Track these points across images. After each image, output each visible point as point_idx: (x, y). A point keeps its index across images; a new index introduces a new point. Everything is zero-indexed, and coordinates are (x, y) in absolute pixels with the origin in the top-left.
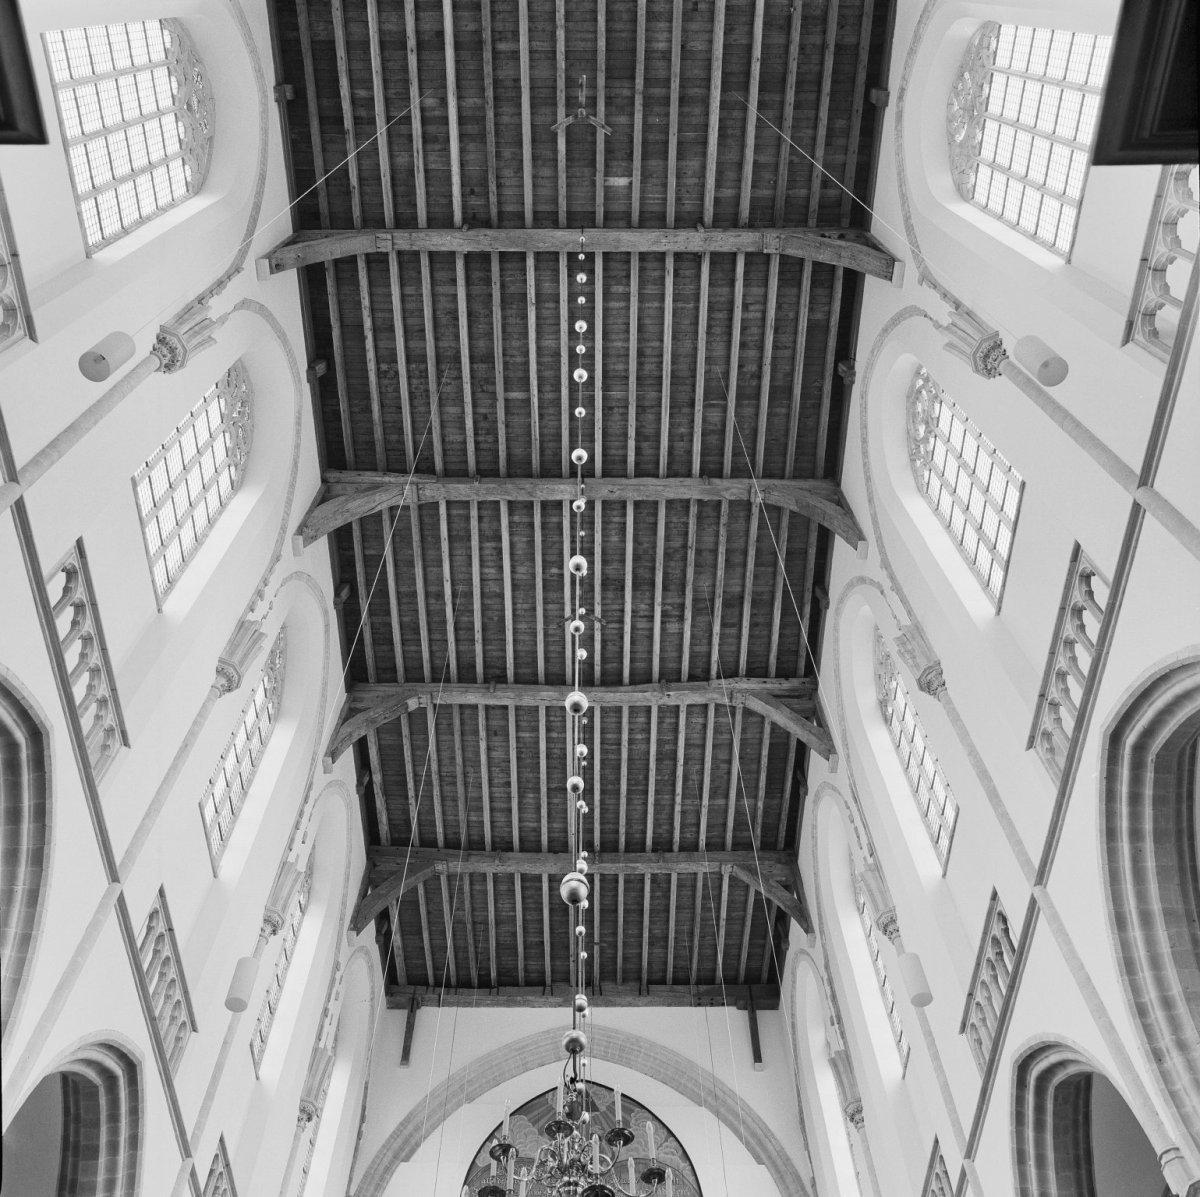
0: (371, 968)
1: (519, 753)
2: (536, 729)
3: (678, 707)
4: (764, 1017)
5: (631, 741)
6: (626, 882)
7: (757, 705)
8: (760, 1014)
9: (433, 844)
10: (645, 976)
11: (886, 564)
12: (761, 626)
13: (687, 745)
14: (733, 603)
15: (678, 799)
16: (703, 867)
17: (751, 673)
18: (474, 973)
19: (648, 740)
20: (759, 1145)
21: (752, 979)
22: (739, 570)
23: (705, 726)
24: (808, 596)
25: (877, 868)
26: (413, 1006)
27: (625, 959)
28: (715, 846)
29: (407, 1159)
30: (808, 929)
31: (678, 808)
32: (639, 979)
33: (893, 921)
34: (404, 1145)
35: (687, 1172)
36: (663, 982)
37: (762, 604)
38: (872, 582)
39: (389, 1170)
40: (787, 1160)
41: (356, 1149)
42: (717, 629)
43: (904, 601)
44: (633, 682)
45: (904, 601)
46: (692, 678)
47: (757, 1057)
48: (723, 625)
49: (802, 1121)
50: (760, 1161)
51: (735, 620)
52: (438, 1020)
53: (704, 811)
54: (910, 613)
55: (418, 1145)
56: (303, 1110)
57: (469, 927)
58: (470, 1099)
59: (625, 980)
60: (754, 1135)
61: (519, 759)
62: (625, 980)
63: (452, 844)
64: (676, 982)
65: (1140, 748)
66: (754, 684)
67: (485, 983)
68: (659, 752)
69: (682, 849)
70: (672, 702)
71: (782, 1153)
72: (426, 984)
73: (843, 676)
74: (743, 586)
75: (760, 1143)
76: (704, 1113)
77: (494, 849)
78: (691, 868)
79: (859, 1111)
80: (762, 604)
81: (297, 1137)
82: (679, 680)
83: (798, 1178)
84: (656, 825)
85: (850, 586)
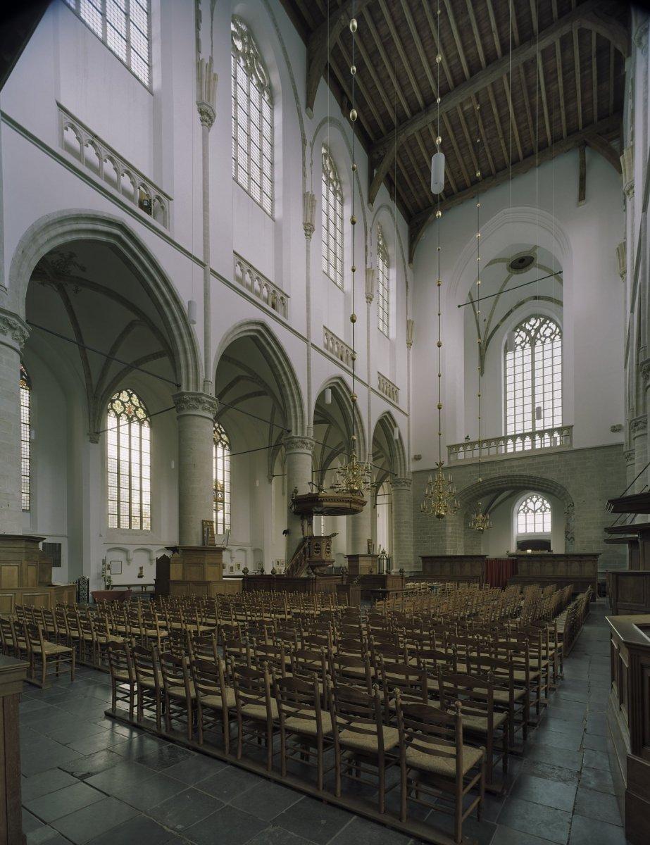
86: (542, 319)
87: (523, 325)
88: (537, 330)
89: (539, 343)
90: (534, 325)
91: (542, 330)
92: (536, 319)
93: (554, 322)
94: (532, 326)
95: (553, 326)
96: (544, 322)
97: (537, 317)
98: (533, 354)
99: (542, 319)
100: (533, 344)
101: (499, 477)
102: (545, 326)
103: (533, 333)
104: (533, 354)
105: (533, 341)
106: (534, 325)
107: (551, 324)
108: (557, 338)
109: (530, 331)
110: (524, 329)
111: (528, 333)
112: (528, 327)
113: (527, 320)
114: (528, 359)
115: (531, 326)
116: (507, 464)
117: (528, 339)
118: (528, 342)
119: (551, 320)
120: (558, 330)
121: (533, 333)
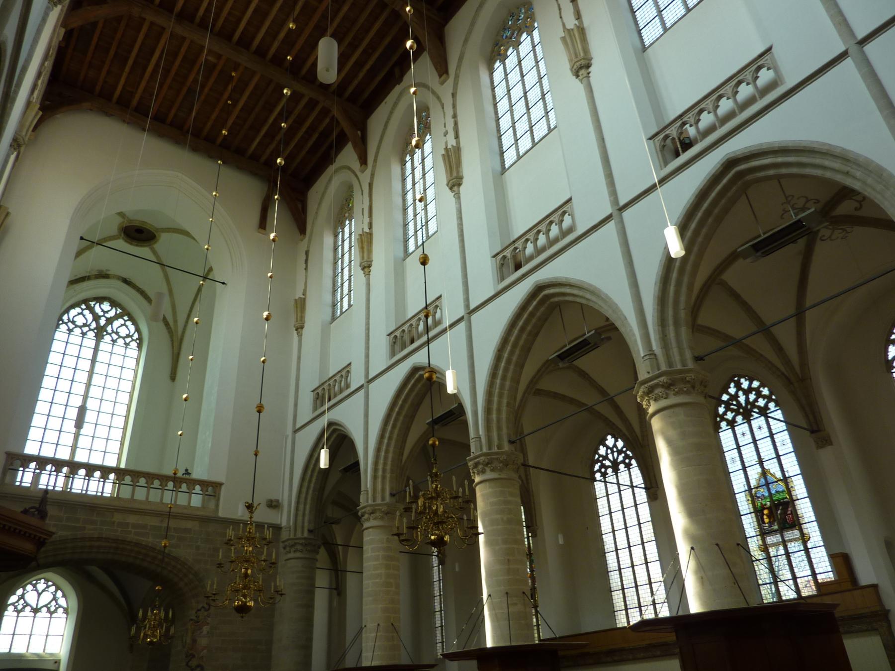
86: (119, 311)
87: (92, 304)
88: (110, 321)
89: (107, 338)
90: (107, 312)
91: (117, 324)
92: (112, 306)
93: (135, 323)
94: (105, 312)
95: (132, 328)
96: (117, 317)
97: (114, 304)
98: (96, 350)
99: (119, 311)
100: (99, 337)
101: (99, 539)
102: (121, 321)
103: (103, 322)
104: (96, 350)
105: (100, 333)
106: (107, 312)
107: (129, 323)
108: (134, 345)
109: (100, 317)
110: (92, 311)
111: (96, 318)
112: (97, 309)
113: (100, 300)
114: (88, 353)
115: (103, 311)
116: (118, 518)
117: (94, 325)
118: (93, 330)
119: (131, 319)
120: (136, 336)
121: (103, 322)
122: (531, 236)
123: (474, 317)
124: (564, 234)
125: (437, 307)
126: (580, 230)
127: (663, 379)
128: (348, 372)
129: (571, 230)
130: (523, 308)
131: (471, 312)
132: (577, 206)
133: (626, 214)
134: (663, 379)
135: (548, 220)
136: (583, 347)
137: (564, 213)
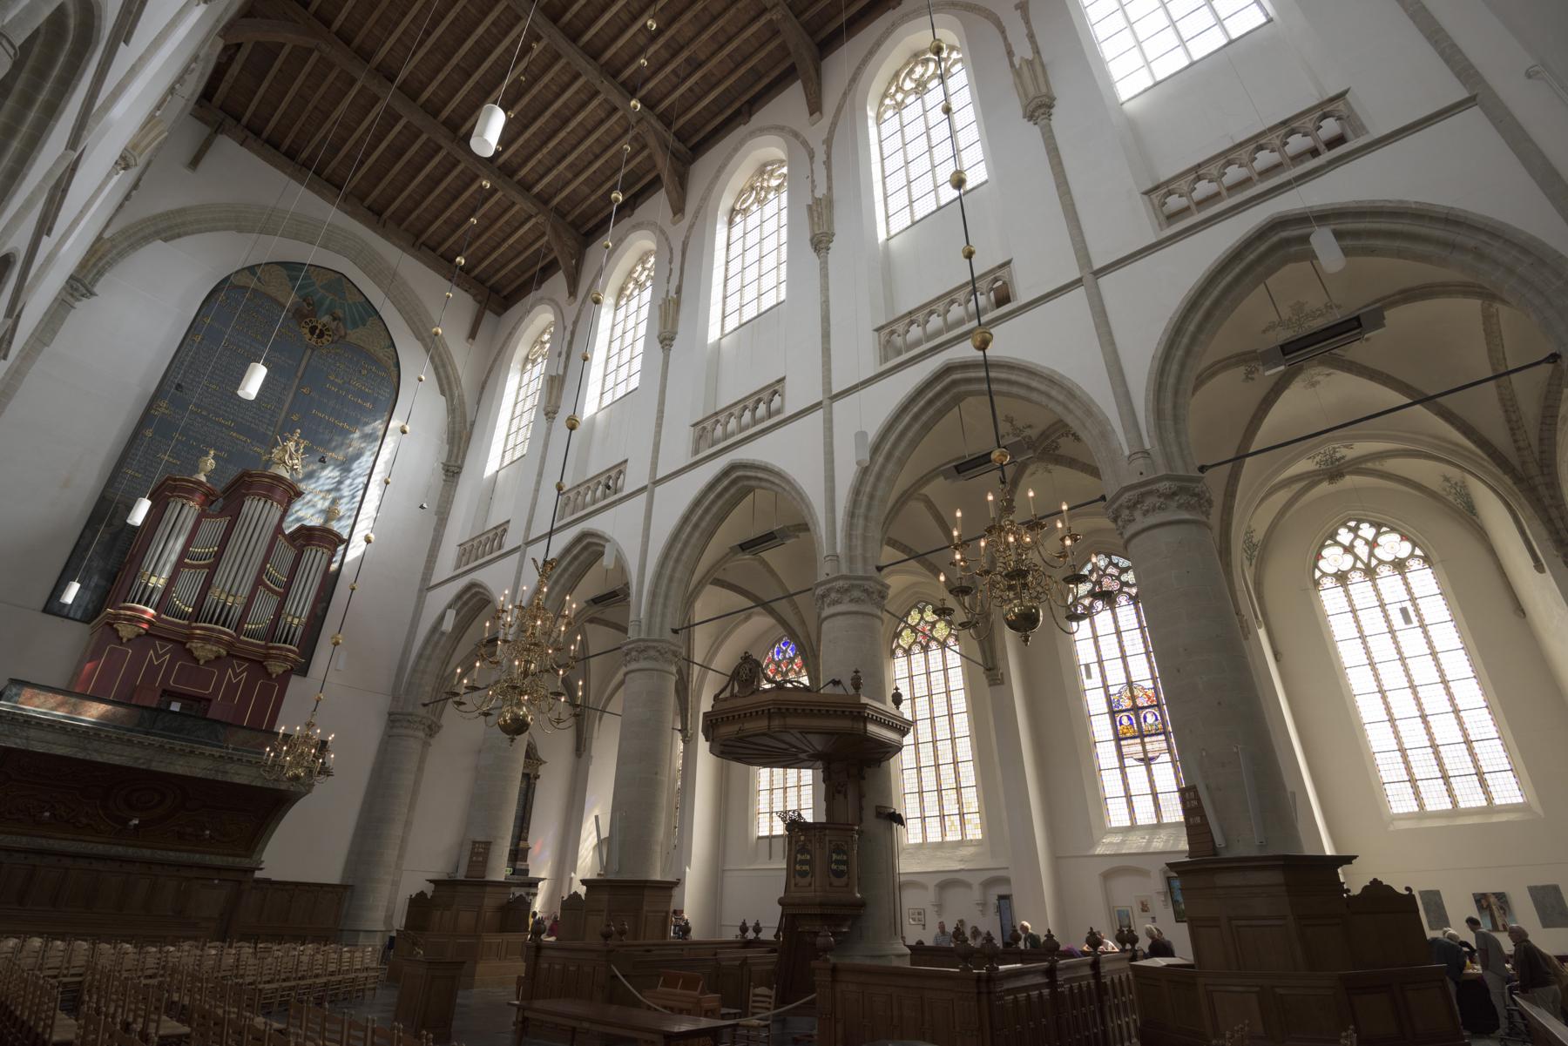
0: (202, 74)
1: (456, 19)
2: (485, 14)
3: (597, 93)
4: (489, 316)
5: (546, 86)
6: (462, 172)
7: (652, 141)
8: (488, 313)
9: (328, 24)
10: (424, 237)
11: (828, 142)
12: (695, 96)
13: (581, 123)
14: (695, 65)
15: (545, 151)
16: (522, 205)
17: (661, 117)
18: (288, 142)
19: (558, 96)
20: (446, 383)
21: (494, 290)
22: (716, 46)
23: (602, 122)
24: (736, 105)
25: (678, 303)
26: (218, 129)
27: (418, 217)
28: (543, 200)
29: (166, 240)
30: (573, 292)
31: (539, 156)
32: (417, 237)
33: (672, 339)
34: (169, 228)
35: (395, 374)
36: (434, 250)
37: (709, 84)
38: (805, 143)
39: (147, 239)
40: (462, 403)
41: (121, 206)
42: (668, 69)
43: (829, 178)
44: (583, 48)
45: (829, 178)
46: (623, 84)
47: (472, 335)
48: (674, 71)
49: (483, 388)
50: (443, 393)
51: (682, 75)
52: (230, 152)
53: (555, 172)
54: (830, 188)
55: (179, 236)
56: (123, 157)
57: (310, 107)
58: (240, 230)
59: (406, 230)
60: (448, 377)
61: (452, 22)
62: (406, 230)
63: (345, 38)
64: (442, 256)
65: (955, 383)
66: (659, 126)
67: (291, 155)
68: (558, 111)
69: (519, 182)
70: (598, 86)
71: (461, 397)
72: (238, 120)
73: (723, 176)
74: (708, 59)
75: (449, 383)
76: (419, 344)
77: (377, 69)
78: (518, 198)
79: (555, 412)
80: (709, 84)
81: (109, 176)
82: (614, 76)
83: (464, 415)
84: (515, 154)
85: (779, 129)
122: (736, 411)
123: (658, 489)
124: (770, 415)
125: (620, 472)
126: (788, 412)
127: (840, 583)
128: (505, 530)
129: (779, 411)
130: (711, 486)
131: (657, 483)
132: (789, 388)
133: (837, 405)
134: (840, 583)
135: (756, 398)
136: (768, 539)
137: (775, 392)
